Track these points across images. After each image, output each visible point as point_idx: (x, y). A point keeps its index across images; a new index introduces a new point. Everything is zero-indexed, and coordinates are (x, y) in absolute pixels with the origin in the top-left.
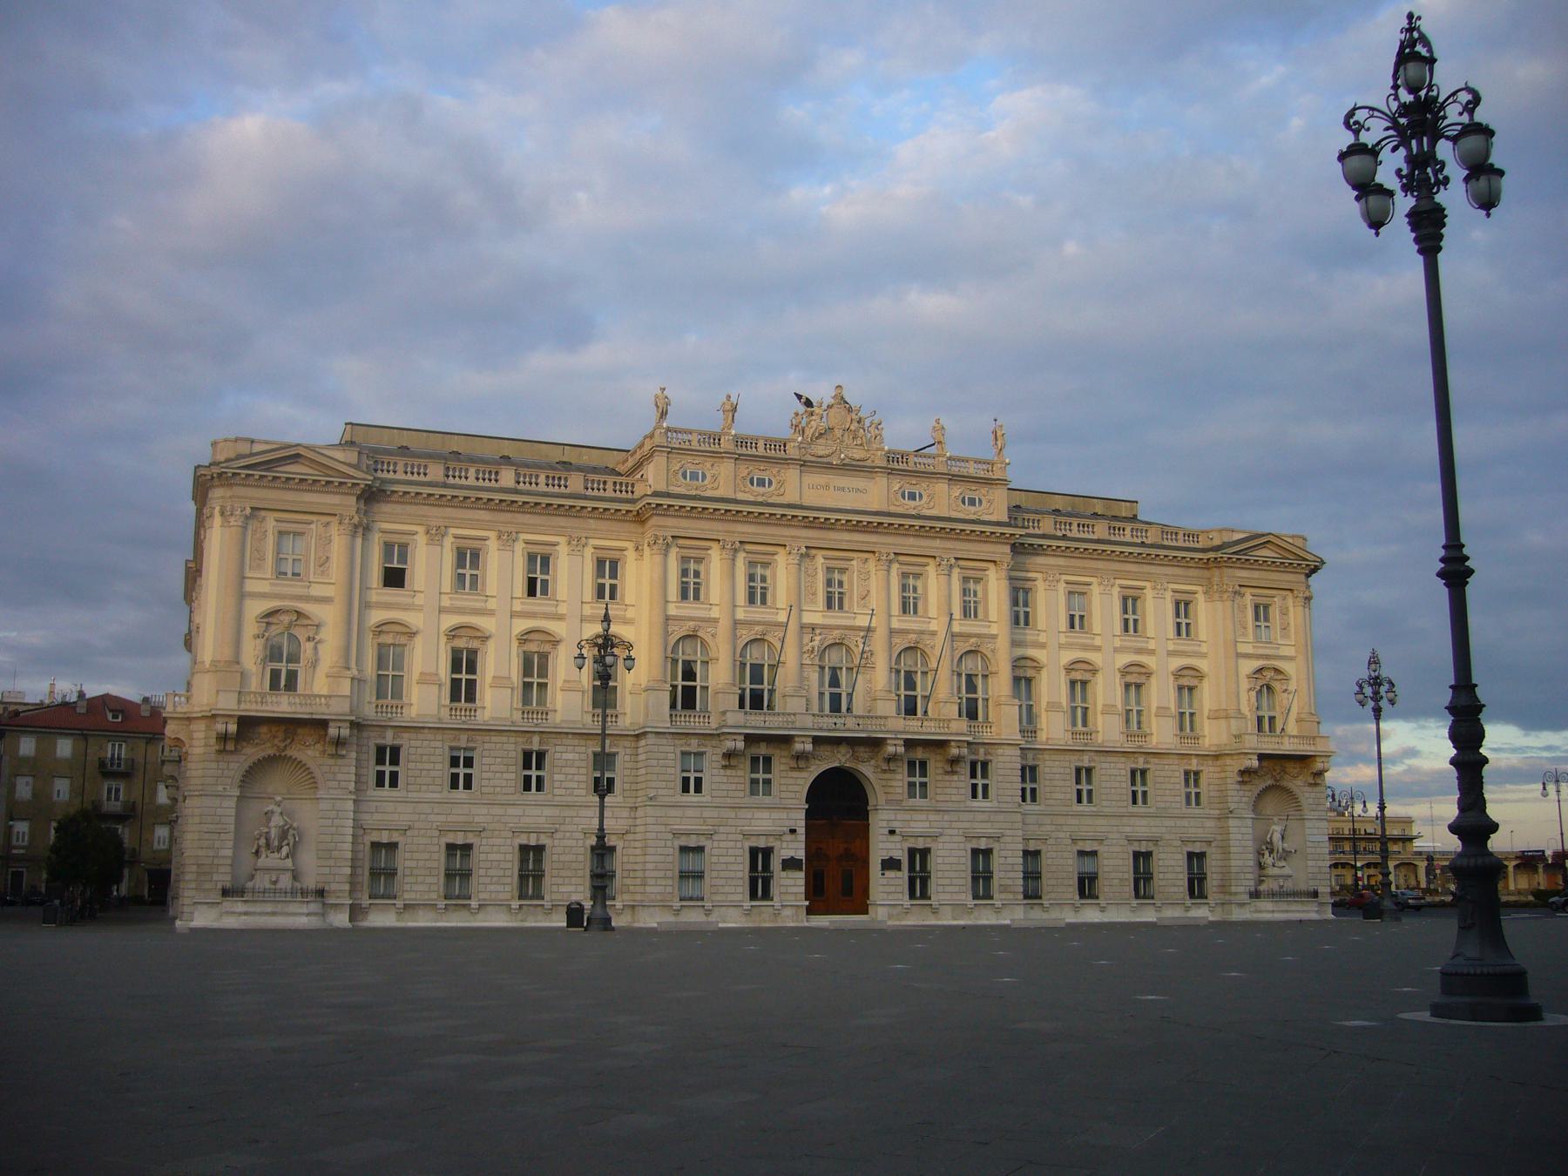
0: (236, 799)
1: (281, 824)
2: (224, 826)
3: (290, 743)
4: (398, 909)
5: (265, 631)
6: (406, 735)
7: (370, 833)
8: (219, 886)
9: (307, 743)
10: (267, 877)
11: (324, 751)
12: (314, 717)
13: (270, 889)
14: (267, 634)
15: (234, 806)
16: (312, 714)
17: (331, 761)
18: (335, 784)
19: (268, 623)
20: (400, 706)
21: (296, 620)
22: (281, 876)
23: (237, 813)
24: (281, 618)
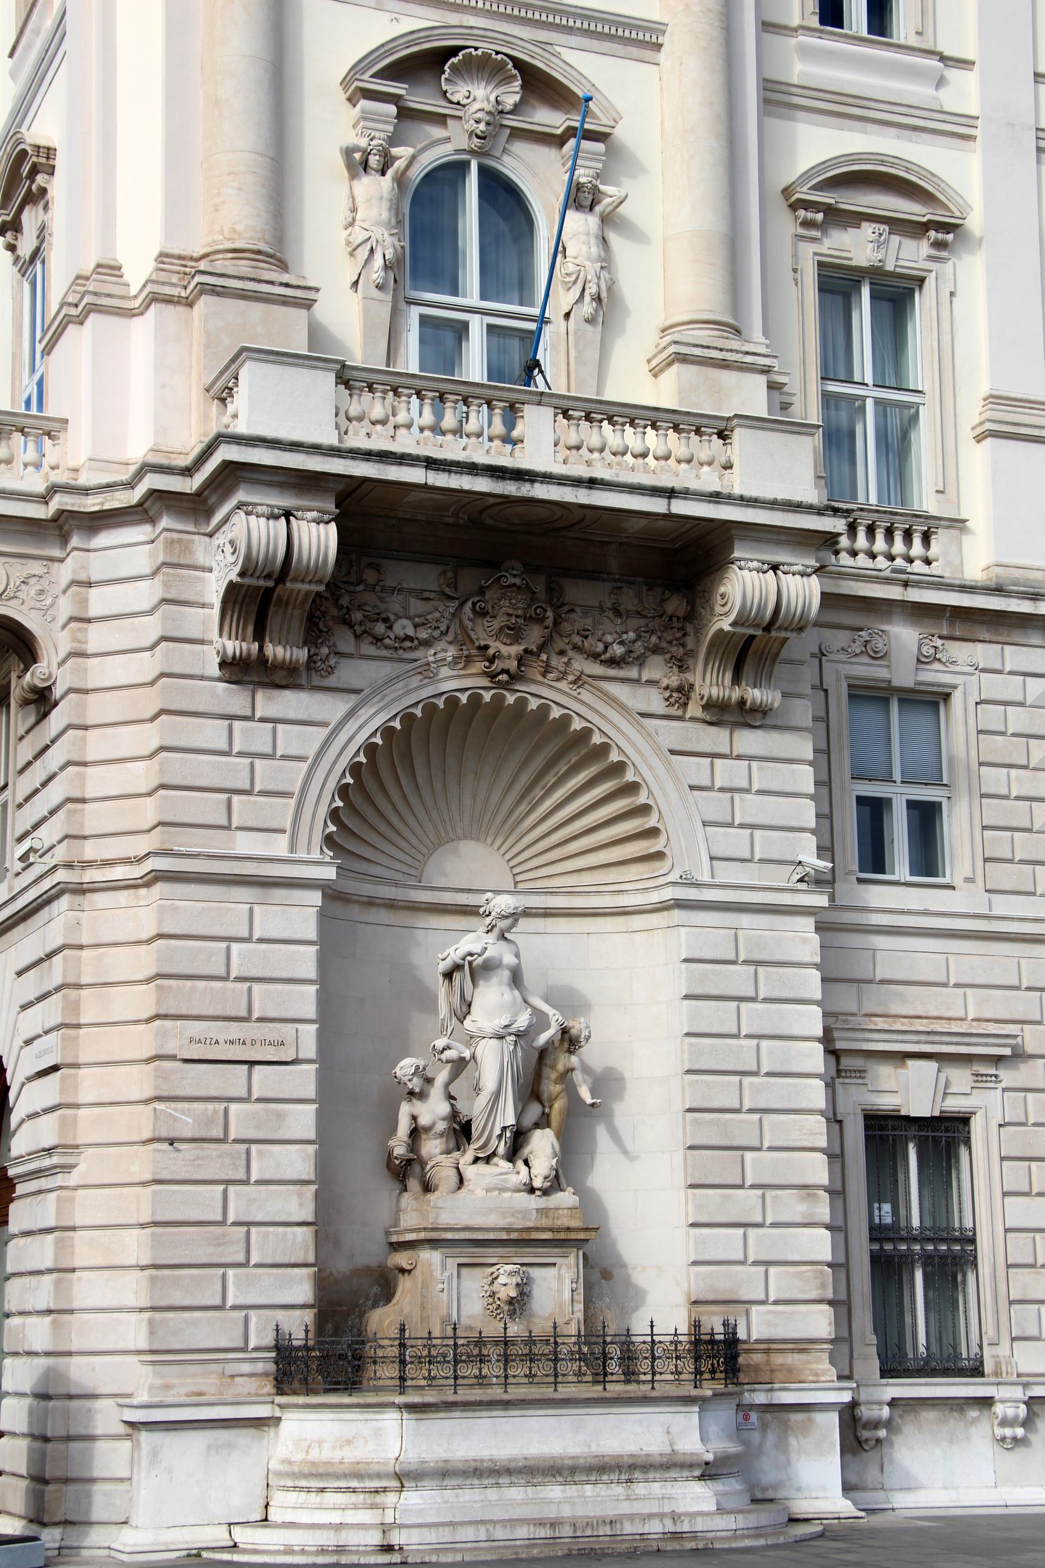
0: (316, 898)
1: (523, 1021)
2: (270, 1031)
3: (541, 648)
4: (1004, 1423)
5: (394, 140)
6: (962, 653)
7: (861, 1073)
8: (260, 1335)
9: (618, 650)
10: (474, 1283)
11: (682, 693)
12: (681, 507)
13: (480, 1342)
14: (403, 152)
15: (312, 934)
16: (671, 493)
17: (716, 738)
18: (735, 842)
19: (405, 114)
20: (901, 526)
21: (516, 109)
22: (535, 1273)
23: (323, 962)
24: (459, 91)
